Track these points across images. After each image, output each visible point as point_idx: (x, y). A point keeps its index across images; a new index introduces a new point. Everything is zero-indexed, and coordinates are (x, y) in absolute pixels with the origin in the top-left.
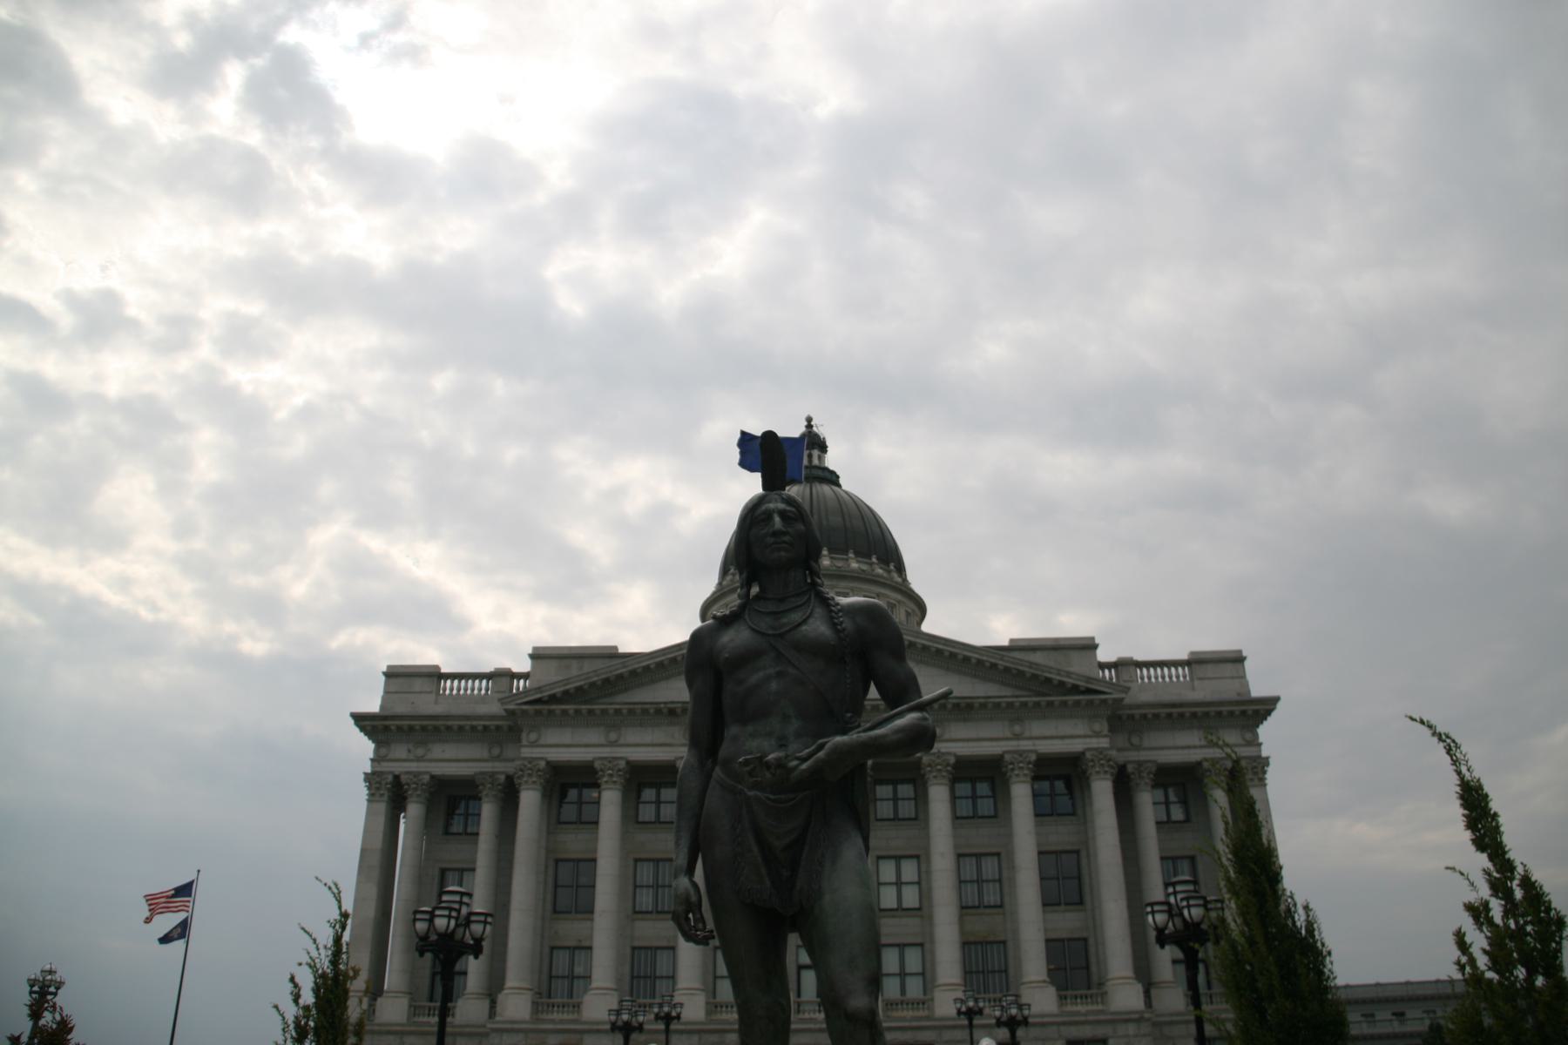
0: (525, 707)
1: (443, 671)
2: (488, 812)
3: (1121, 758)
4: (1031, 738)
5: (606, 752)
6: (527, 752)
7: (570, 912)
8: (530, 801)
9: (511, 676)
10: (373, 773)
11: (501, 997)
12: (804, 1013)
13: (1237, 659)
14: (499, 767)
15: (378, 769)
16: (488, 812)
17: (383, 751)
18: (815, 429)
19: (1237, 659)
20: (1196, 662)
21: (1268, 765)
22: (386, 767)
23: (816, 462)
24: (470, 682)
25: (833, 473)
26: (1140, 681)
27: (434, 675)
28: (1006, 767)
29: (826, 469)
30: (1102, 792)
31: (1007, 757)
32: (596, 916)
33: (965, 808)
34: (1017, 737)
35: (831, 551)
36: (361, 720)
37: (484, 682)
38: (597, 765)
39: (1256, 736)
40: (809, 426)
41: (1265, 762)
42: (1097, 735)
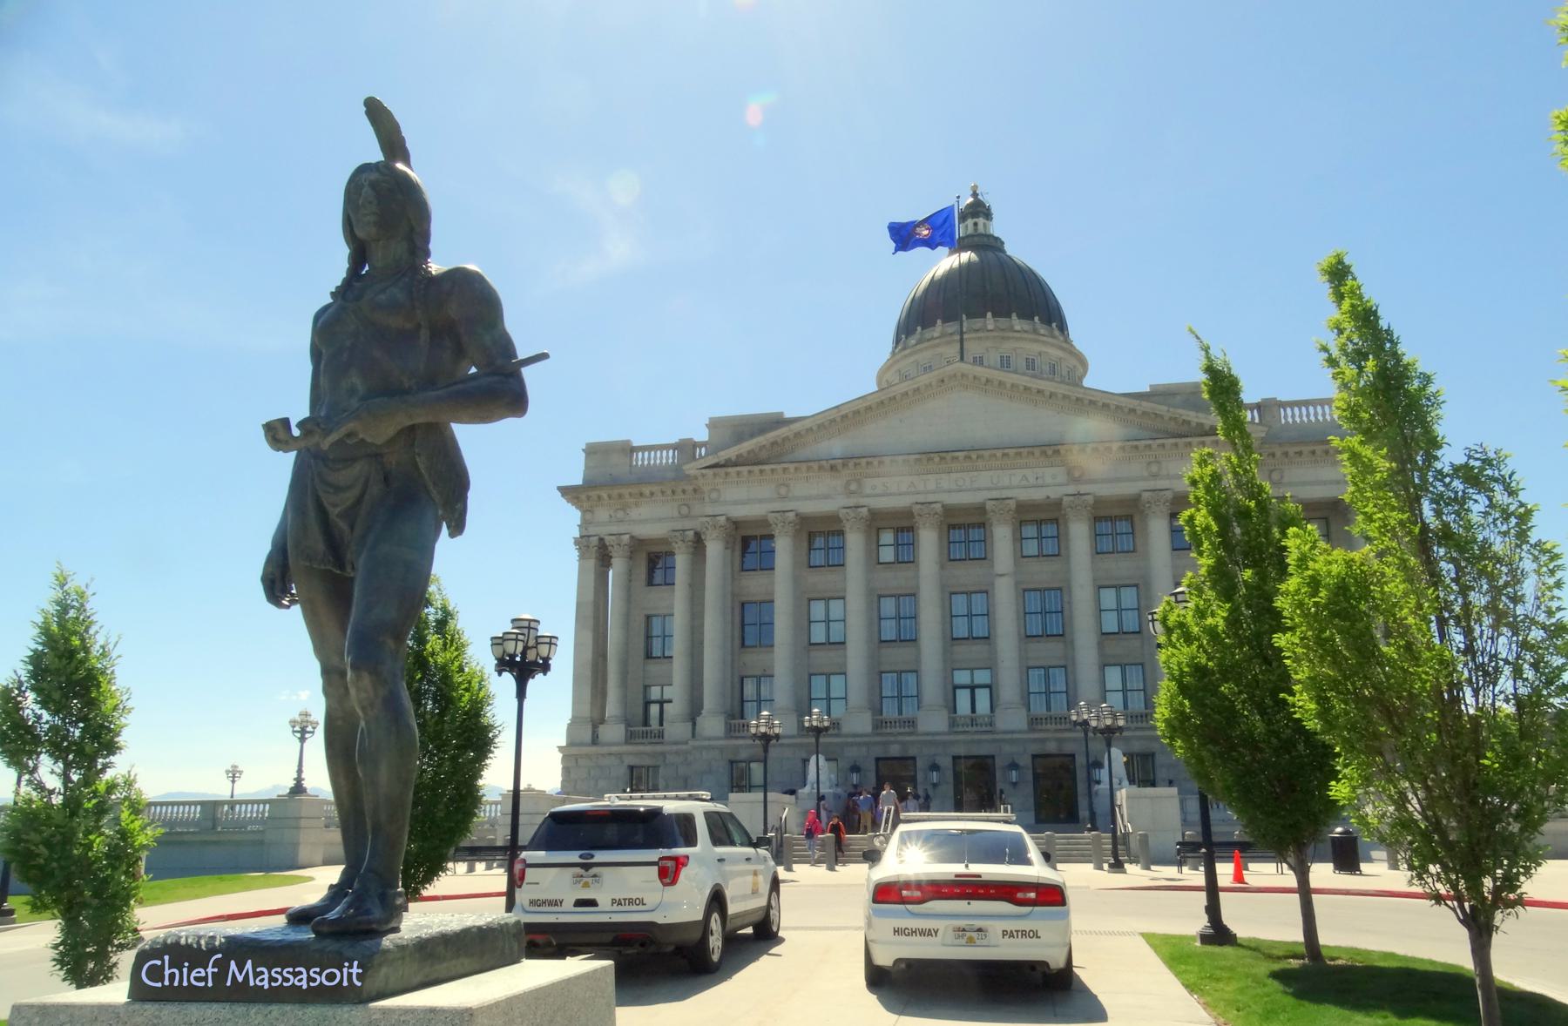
0: (703, 471)
1: (634, 445)
2: (681, 562)
5: (778, 506)
6: (709, 510)
7: (756, 647)
8: (714, 549)
9: (696, 444)
10: (582, 537)
11: (699, 720)
12: (958, 725)
14: (688, 524)
15: (585, 533)
17: (588, 516)
18: (980, 197)
22: (592, 530)
23: (981, 229)
24: (659, 453)
25: (997, 239)
27: (628, 449)
28: (1144, 506)
29: (992, 236)
31: (1146, 495)
32: (776, 649)
34: (1155, 476)
35: (994, 316)
36: (568, 492)
37: (671, 452)
38: (771, 517)
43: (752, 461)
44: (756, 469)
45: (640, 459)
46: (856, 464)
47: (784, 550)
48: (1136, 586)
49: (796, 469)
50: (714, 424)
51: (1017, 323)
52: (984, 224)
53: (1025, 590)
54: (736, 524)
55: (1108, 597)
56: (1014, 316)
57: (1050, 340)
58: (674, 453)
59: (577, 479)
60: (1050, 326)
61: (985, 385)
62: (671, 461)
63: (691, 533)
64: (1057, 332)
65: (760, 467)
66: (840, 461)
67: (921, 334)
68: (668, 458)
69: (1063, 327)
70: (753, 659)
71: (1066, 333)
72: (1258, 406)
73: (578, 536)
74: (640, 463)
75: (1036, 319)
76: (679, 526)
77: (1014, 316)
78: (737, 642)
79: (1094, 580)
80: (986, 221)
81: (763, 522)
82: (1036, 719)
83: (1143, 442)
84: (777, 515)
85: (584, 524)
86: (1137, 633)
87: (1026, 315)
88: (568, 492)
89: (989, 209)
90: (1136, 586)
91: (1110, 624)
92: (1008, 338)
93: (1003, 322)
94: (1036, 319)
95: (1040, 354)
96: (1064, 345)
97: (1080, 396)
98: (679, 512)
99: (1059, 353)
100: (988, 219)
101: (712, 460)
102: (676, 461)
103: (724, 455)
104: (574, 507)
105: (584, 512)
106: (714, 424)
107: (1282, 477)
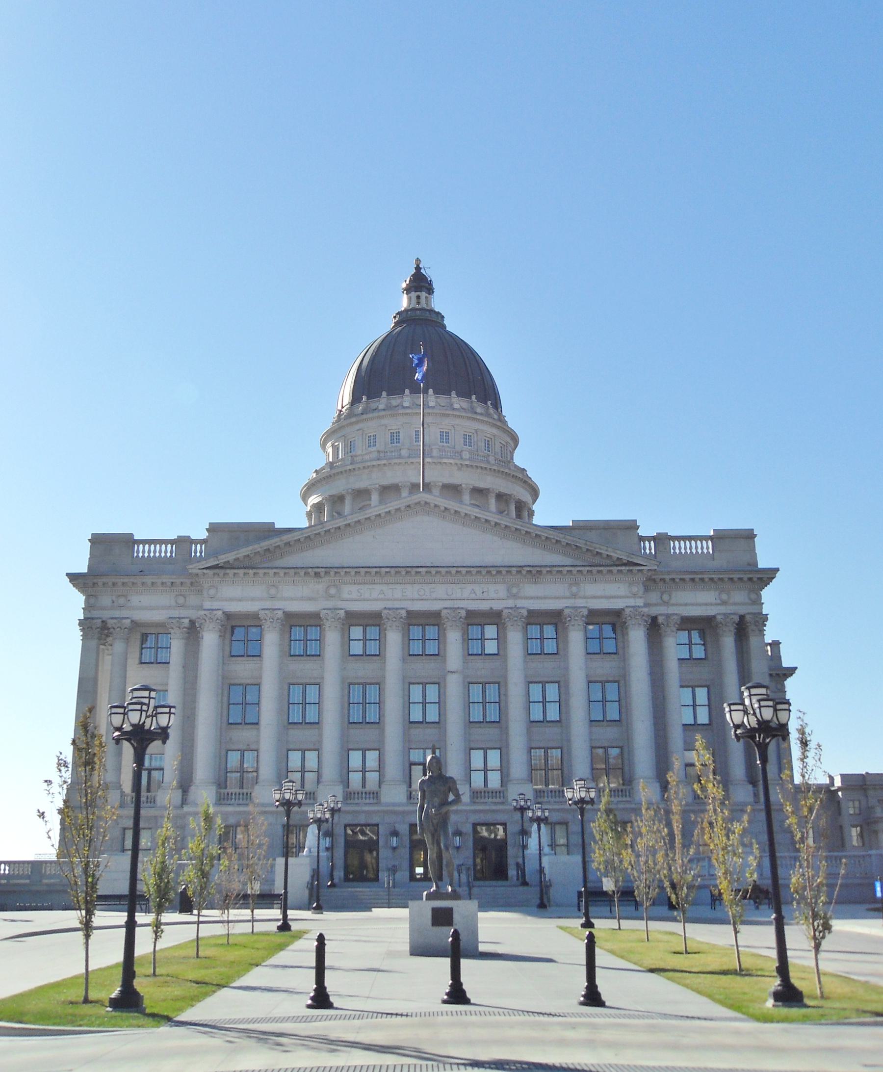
0: (205, 571)
1: (135, 538)
2: (177, 646)
3: (654, 611)
4: (585, 597)
5: (268, 604)
6: (207, 605)
8: (210, 640)
10: (86, 619)
13: (749, 536)
14: (183, 613)
15: (89, 616)
16: (177, 646)
17: (92, 601)
18: (422, 271)
19: (749, 536)
20: (720, 538)
21: (767, 619)
22: (95, 614)
23: (423, 304)
25: (438, 313)
26: (672, 551)
27: (128, 541)
29: (432, 311)
30: (637, 638)
31: (567, 612)
33: (535, 647)
34: (574, 596)
35: (435, 393)
36: (74, 578)
38: (262, 614)
39: (760, 597)
40: (418, 268)
41: (765, 618)
42: (634, 596)
43: (246, 565)
44: (251, 572)
45: (142, 551)
46: (336, 573)
47: (271, 642)
48: (558, 682)
49: (285, 573)
50: (213, 528)
51: (458, 402)
52: (426, 297)
53: (469, 683)
54: (228, 616)
55: (536, 691)
56: (453, 394)
57: (486, 419)
58: (172, 547)
59: (82, 567)
60: (486, 403)
61: (443, 512)
62: (169, 555)
63: (186, 621)
64: (492, 411)
65: (255, 571)
66: (323, 569)
67: (367, 403)
68: (167, 551)
69: (497, 404)
70: (243, 735)
71: (499, 410)
72: (654, 538)
73: (83, 618)
74: (141, 555)
75: (474, 397)
76: (176, 613)
77: (453, 394)
78: (379, 794)
79: (526, 676)
80: (427, 295)
81: (255, 616)
82: (477, 792)
83: (567, 568)
84: (266, 612)
85: (87, 608)
86: (557, 721)
87: (465, 394)
88: (74, 578)
89: (430, 283)
90: (558, 682)
91: (537, 713)
92: (448, 415)
93: (443, 400)
94: (474, 397)
95: (476, 431)
96: (499, 424)
97: (519, 527)
98: (177, 603)
99: (495, 431)
100: (429, 294)
101: (212, 562)
102: (174, 555)
103: (222, 559)
104: (82, 595)
105: (88, 597)
106: (213, 528)
107: (670, 599)
